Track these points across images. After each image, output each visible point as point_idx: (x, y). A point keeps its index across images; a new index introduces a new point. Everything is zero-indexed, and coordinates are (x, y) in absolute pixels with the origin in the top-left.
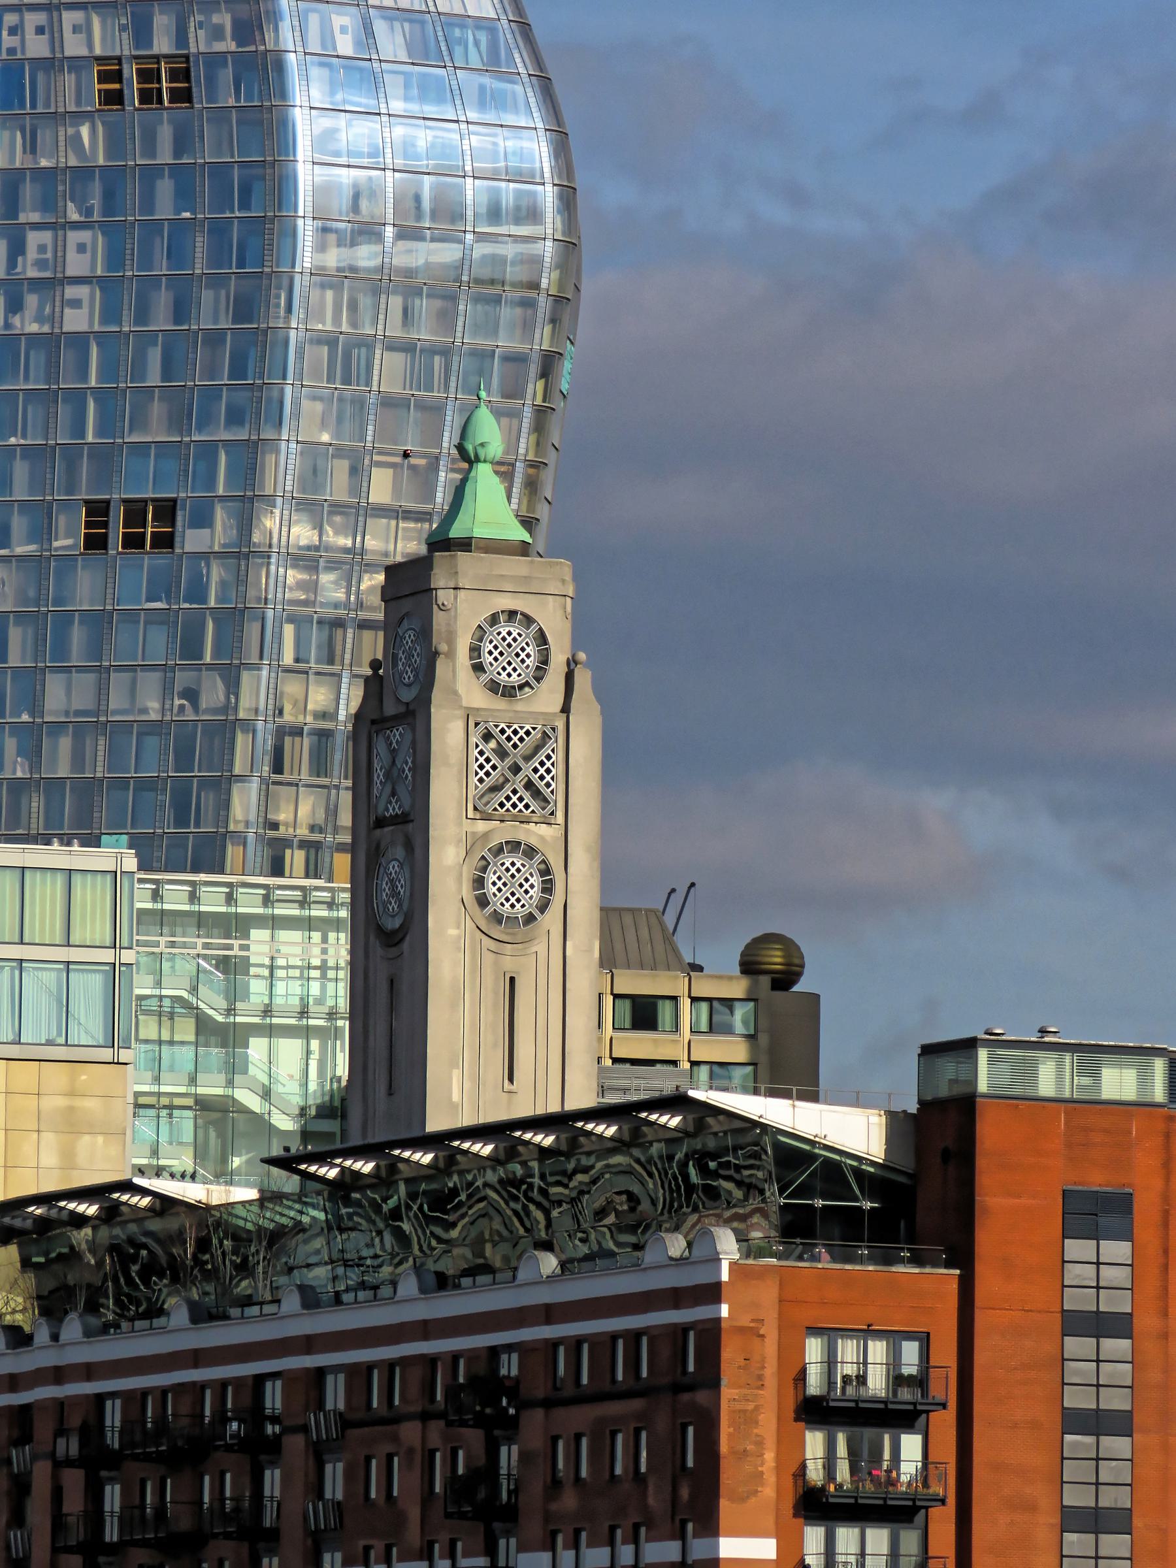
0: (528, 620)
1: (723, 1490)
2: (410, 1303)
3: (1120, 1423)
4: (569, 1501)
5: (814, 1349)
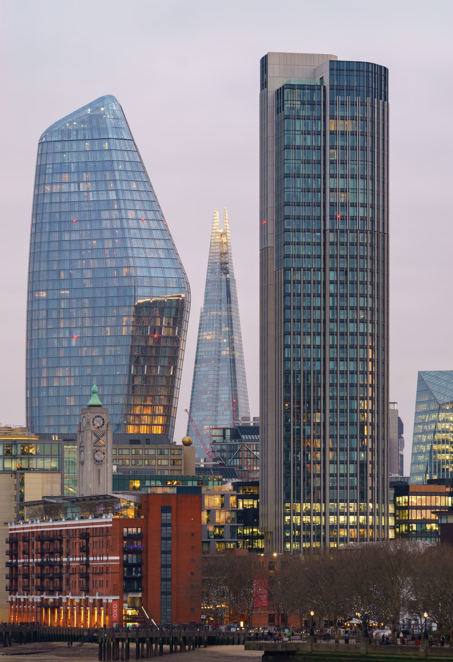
0: (101, 417)
2: (77, 521)
3: (170, 539)
4: (95, 550)
5: (125, 530)
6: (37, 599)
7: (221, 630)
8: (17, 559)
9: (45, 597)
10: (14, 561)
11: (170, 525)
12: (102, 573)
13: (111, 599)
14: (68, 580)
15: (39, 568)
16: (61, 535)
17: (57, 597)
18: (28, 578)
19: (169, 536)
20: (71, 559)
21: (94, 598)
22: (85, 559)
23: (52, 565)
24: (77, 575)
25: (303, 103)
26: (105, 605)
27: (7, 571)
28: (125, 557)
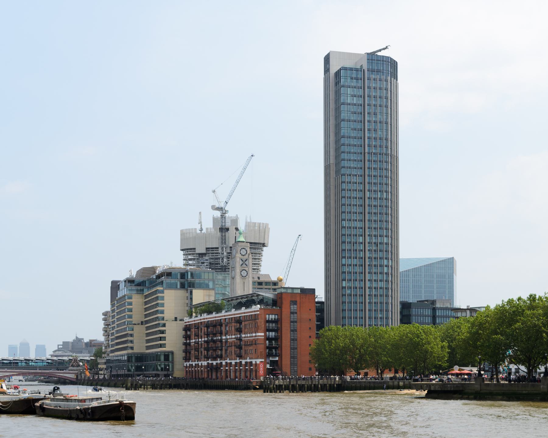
3: (296, 322)
4: (246, 330)
5: (267, 316)
6: (205, 363)
7: (346, 380)
8: (190, 340)
9: (210, 362)
10: (188, 341)
11: (296, 313)
12: (252, 345)
13: (258, 361)
14: (226, 350)
15: (206, 344)
16: (221, 322)
17: (219, 362)
18: (198, 351)
19: (295, 320)
20: (228, 337)
21: (246, 361)
22: (239, 336)
23: (214, 342)
24: (233, 347)
25: (352, 78)
26: (254, 366)
27: (183, 347)
28: (268, 333)
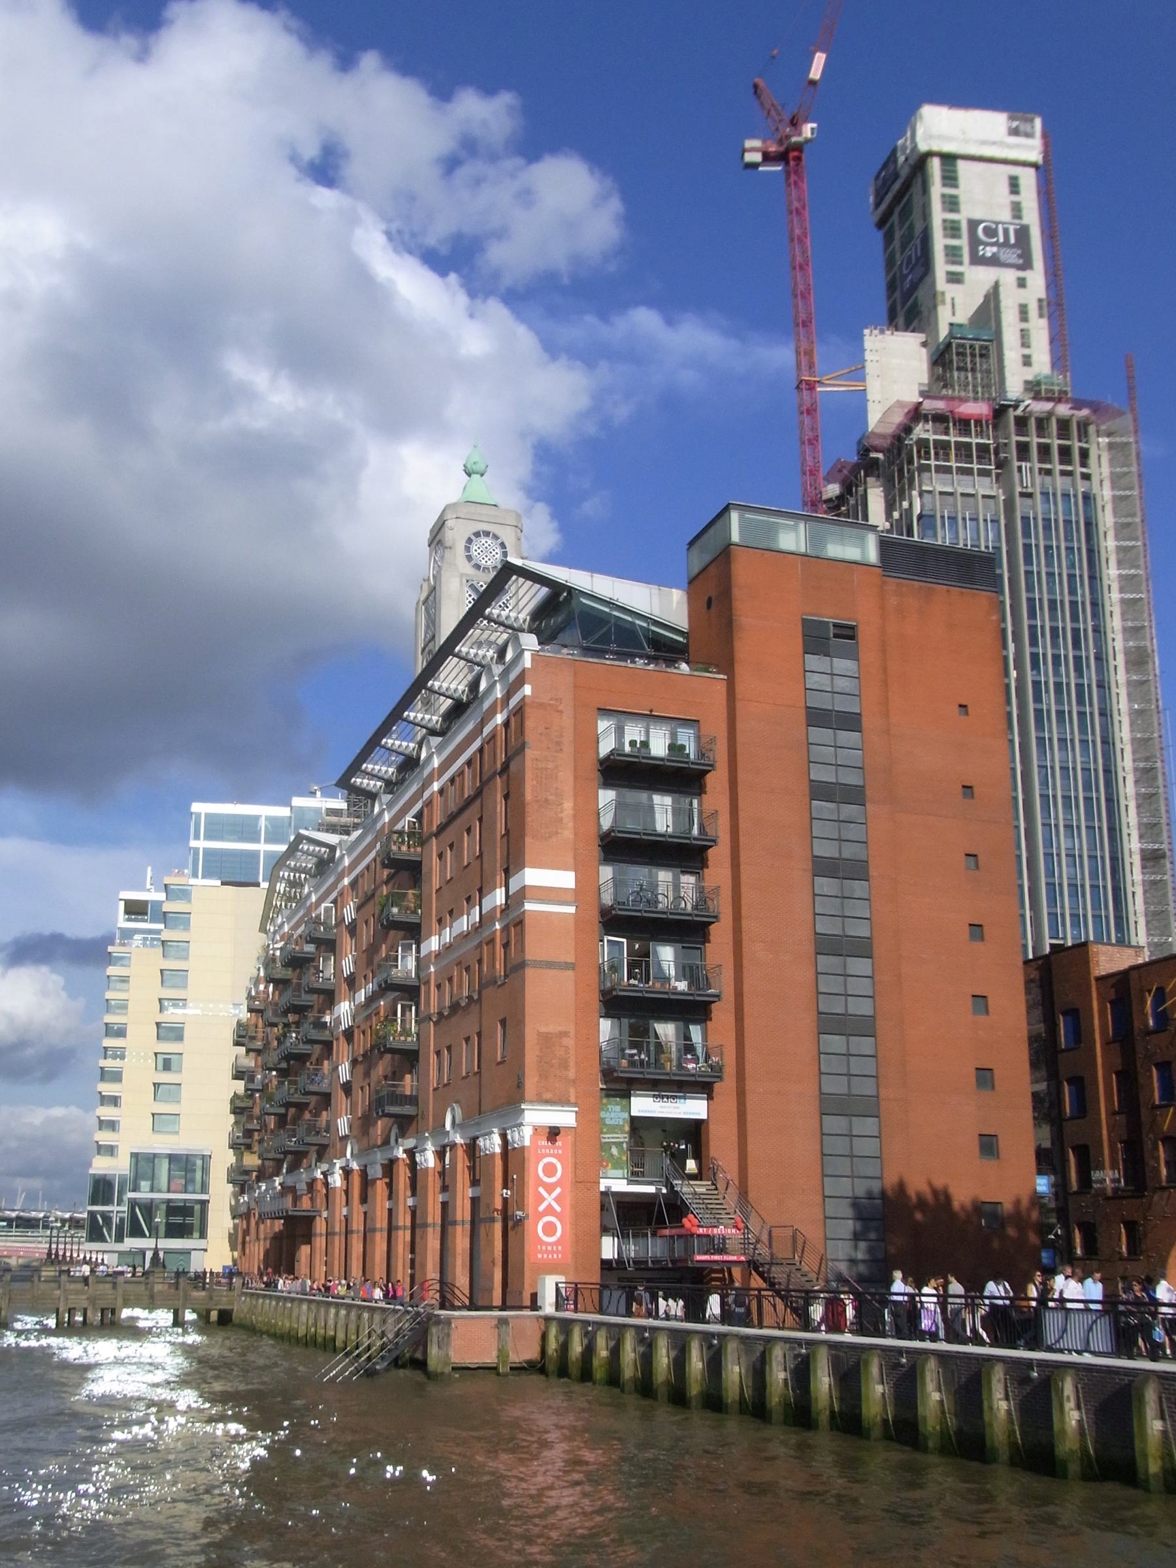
0: (496, 537)
1: (528, 830)
